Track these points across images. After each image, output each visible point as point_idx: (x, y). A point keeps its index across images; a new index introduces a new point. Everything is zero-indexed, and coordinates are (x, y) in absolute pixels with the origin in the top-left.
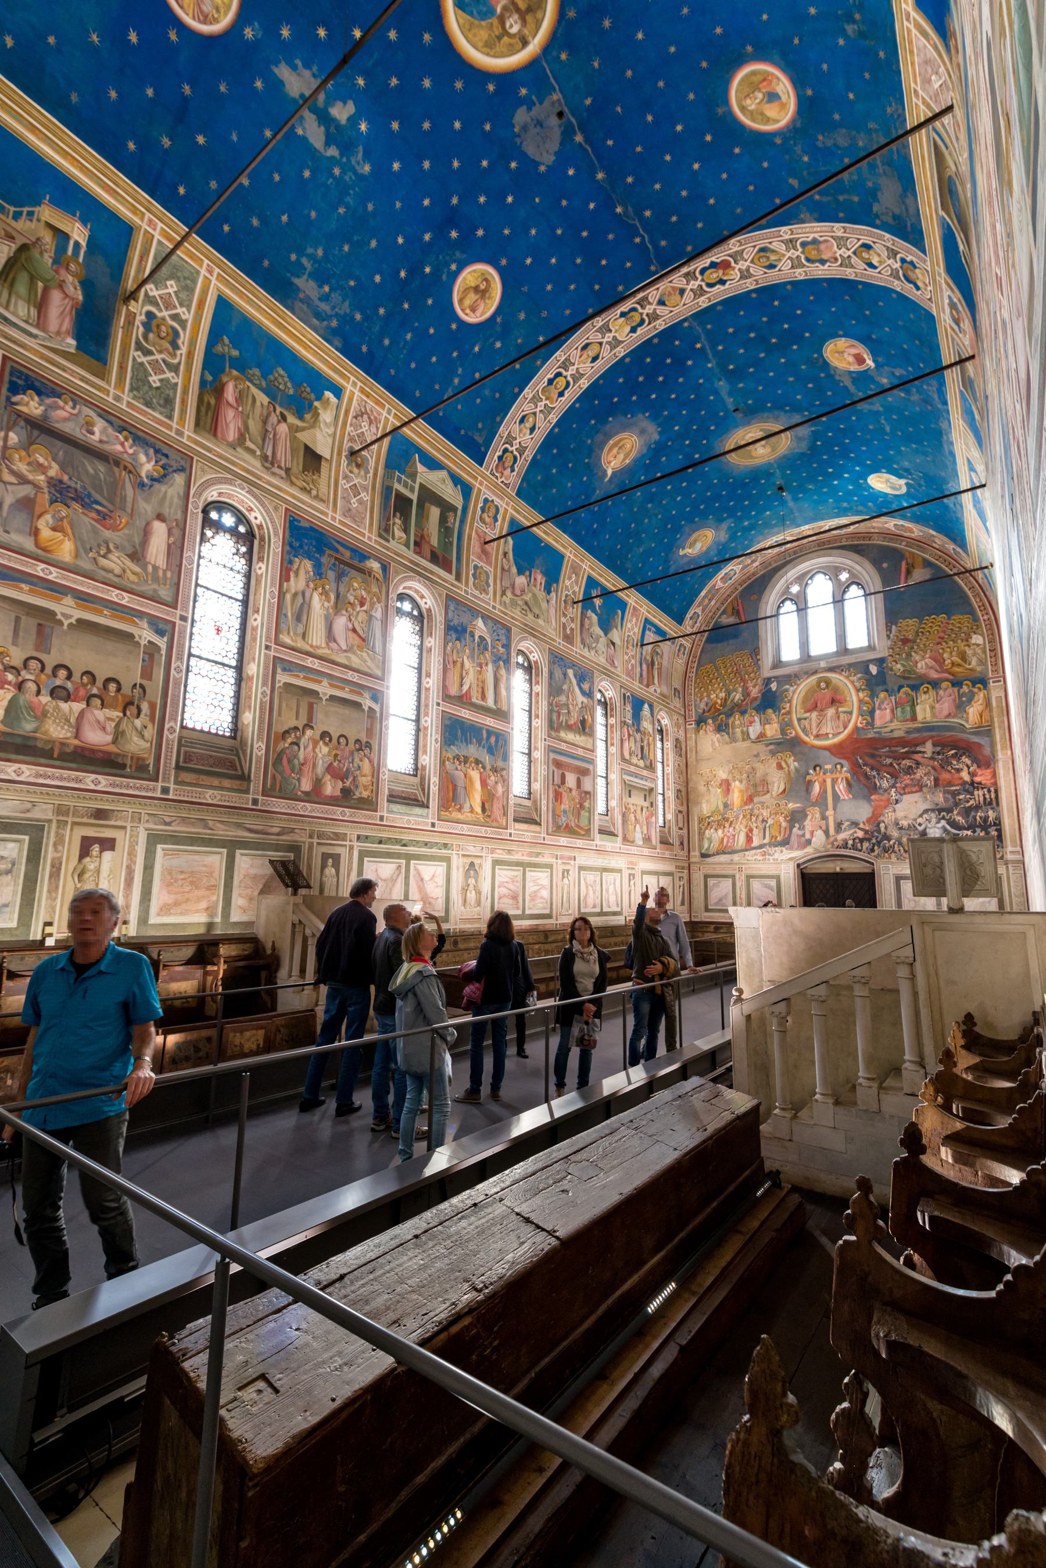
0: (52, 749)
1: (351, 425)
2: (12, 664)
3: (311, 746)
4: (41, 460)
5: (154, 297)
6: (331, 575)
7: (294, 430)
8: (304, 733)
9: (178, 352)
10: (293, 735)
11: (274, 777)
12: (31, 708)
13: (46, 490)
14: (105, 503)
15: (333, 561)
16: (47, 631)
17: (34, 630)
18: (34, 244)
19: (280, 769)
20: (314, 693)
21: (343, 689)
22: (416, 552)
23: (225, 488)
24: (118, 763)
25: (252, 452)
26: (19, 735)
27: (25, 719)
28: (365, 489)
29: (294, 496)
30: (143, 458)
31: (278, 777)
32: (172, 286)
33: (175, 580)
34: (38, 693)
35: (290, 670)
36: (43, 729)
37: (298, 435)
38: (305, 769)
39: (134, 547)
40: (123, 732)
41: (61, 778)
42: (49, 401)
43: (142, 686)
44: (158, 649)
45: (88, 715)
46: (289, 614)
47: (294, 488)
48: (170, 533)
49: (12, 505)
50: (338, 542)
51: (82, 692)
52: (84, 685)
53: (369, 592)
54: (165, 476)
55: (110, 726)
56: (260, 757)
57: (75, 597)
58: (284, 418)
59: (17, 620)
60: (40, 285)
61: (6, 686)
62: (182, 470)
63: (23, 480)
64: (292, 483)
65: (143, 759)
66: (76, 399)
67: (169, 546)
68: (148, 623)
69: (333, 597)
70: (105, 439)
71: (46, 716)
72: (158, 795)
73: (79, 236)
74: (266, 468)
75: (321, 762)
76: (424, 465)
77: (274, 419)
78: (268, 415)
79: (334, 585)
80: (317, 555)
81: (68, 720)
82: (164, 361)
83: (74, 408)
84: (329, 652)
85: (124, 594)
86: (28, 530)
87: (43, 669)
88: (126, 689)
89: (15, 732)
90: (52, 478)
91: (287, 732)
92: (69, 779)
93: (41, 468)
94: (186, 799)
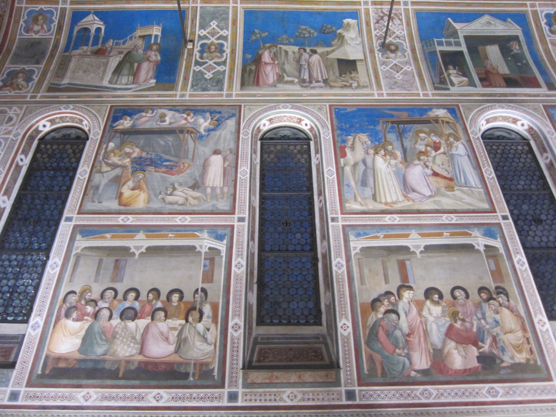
0: (118, 369)
1: (375, 29)
2: (92, 298)
3: (414, 311)
4: (128, 150)
5: (205, 35)
6: (392, 137)
7: (323, 56)
8: (400, 296)
9: (225, 54)
10: (386, 302)
11: (371, 359)
12: (103, 332)
13: (130, 167)
14: (172, 159)
15: (390, 125)
16: (122, 263)
17: (111, 266)
18: (133, 49)
19: (378, 346)
20: (405, 249)
21: (440, 235)
22: (484, 86)
23: (272, 114)
24: (180, 373)
25: (292, 82)
26: (91, 360)
27: (98, 343)
28: (408, 63)
29: (335, 95)
30: (201, 120)
31: (378, 357)
32: (214, 24)
33: (232, 191)
34: (110, 317)
35: (365, 234)
36: (112, 350)
37: (332, 56)
38: (414, 340)
39: (195, 179)
40: (186, 340)
41: (124, 398)
42: (136, 117)
43: (204, 290)
44: (218, 252)
45: (153, 330)
46: (353, 183)
47: (334, 89)
48: (225, 160)
49: (107, 185)
50: (391, 110)
51: (148, 309)
52: (149, 302)
53: (440, 135)
54: (219, 125)
55: (173, 336)
56: (348, 338)
57: (145, 231)
58: (314, 52)
59: (100, 262)
60: (136, 64)
61: (86, 318)
62: (234, 115)
63: (114, 166)
64: (331, 87)
65: (207, 364)
66: (152, 107)
67: (225, 169)
68: (208, 232)
69: (399, 154)
70: (173, 121)
71: (114, 337)
72: (225, 403)
73: (157, 31)
74: (305, 87)
75: (434, 327)
76: (461, 22)
77: (306, 56)
78: (301, 55)
79: (397, 144)
80: (372, 127)
81: (134, 338)
82: (215, 63)
83: (152, 113)
84: (410, 203)
85: (186, 216)
86: (115, 196)
87: (115, 297)
88: (188, 297)
89: (88, 358)
90: (135, 158)
91: (376, 302)
92: (132, 398)
93: (128, 155)
94: (258, 404)
